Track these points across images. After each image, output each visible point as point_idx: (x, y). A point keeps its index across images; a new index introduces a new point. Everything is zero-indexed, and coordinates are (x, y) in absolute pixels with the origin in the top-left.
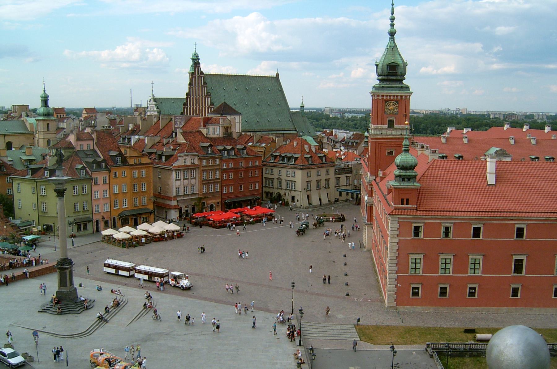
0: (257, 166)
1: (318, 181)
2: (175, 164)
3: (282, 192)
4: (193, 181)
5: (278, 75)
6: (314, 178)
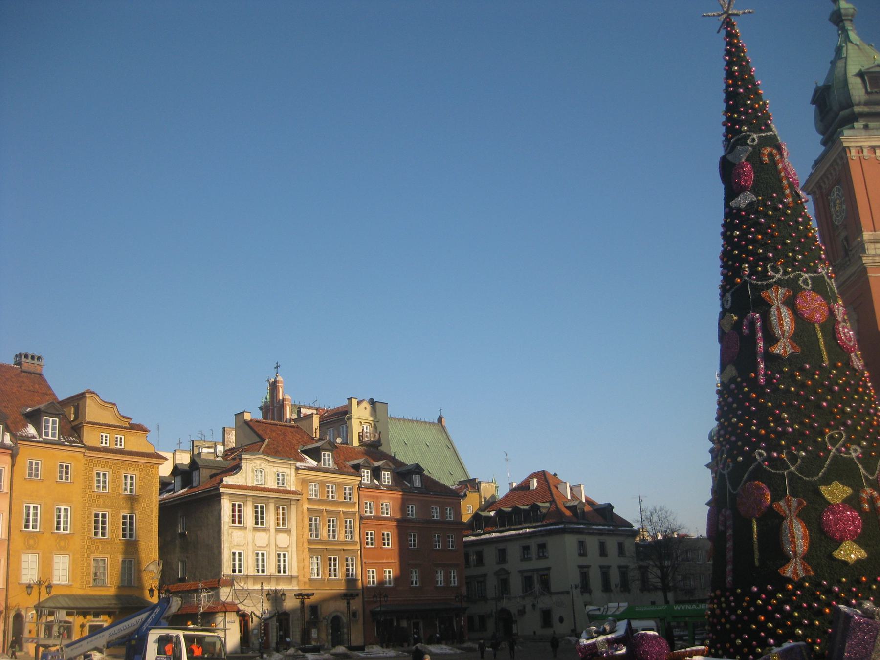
0: (449, 523)
1: (605, 572)
2: (228, 480)
3: (512, 606)
4: (283, 539)
5: (440, 420)
6: (593, 559)
